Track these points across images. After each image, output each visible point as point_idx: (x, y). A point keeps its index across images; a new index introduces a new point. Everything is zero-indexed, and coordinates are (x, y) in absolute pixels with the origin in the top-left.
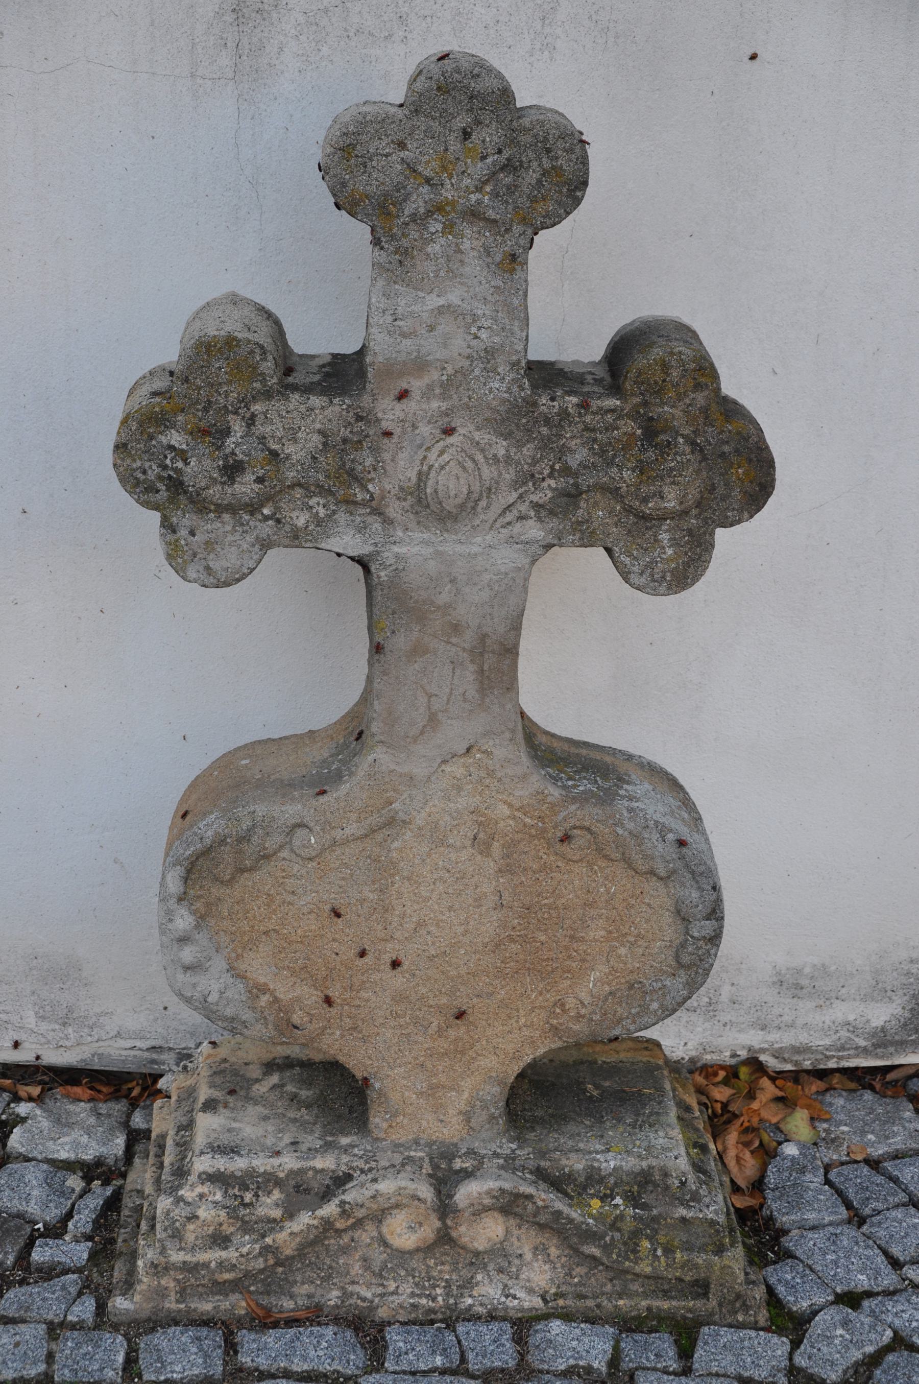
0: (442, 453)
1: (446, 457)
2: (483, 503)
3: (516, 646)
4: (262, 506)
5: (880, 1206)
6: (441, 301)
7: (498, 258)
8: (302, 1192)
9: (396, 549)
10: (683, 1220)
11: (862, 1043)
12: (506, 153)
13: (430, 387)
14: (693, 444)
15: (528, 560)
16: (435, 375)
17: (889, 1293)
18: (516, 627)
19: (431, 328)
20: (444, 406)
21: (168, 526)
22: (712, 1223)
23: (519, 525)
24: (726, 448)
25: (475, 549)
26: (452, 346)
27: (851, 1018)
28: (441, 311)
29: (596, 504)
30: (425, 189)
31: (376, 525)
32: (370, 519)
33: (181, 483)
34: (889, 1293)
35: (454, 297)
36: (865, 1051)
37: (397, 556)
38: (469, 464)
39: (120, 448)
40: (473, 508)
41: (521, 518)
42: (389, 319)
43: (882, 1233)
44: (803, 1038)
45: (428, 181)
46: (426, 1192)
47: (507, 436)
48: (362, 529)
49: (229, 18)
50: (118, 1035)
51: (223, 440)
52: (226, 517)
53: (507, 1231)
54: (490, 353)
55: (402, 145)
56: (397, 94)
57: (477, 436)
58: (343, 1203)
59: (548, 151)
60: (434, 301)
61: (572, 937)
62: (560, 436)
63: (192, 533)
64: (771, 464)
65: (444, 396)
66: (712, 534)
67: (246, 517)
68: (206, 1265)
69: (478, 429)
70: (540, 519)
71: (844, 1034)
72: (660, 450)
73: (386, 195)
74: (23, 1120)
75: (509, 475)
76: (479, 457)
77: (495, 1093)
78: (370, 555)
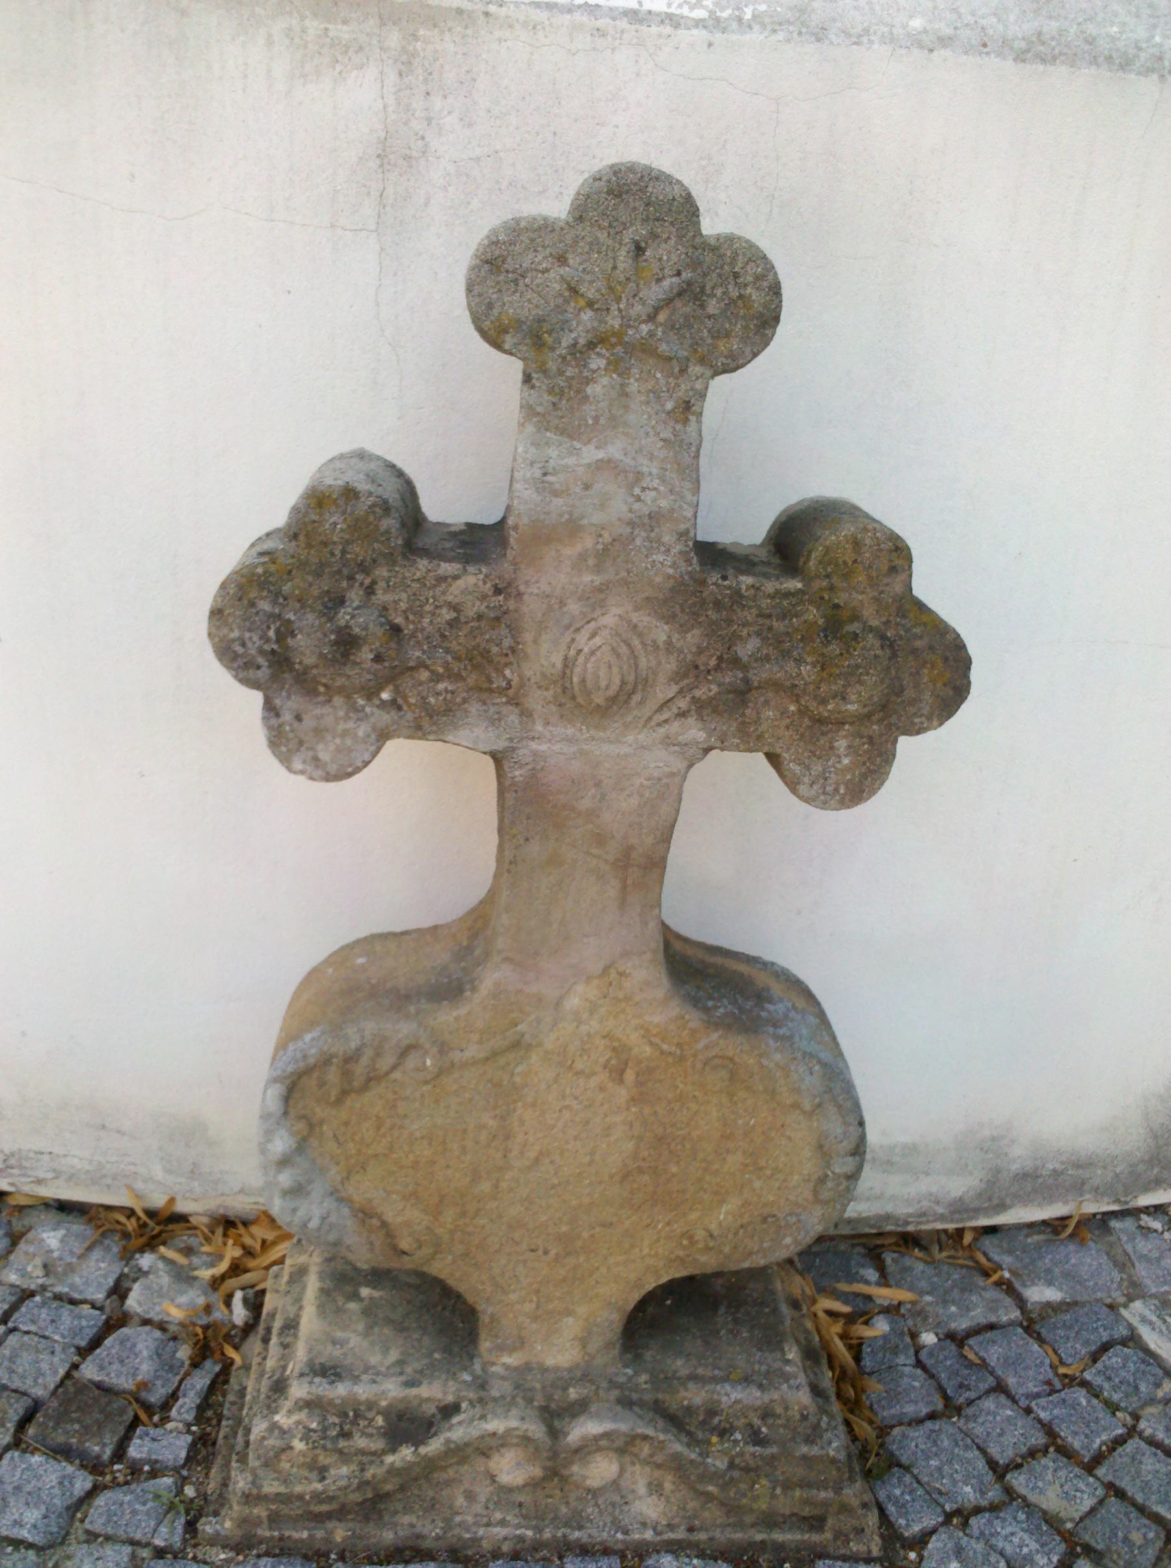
0: (593, 635)
1: (597, 641)
2: (637, 698)
3: (664, 859)
4: (381, 689)
5: (972, 1395)
6: (601, 455)
7: (669, 406)
8: (407, 1426)
9: (534, 745)
10: (805, 1458)
11: (940, 1210)
12: (687, 275)
13: (583, 557)
14: (883, 637)
15: (685, 764)
16: (589, 542)
17: (993, 1508)
18: (666, 838)
19: (587, 487)
20: (598, 580)
21: (270, 708)
22: (833, 1461)
23: (676, 724)
24: (918, 644)
25: (625, 750)
26: (614, 507)
27: (934, 1189)
28: (600, 466)
29: (767, 702)
30: (587, 316)
31: (513, 717)
32: (505, 710)
33: (287, 660)
34: (993, 1508)
35: (614, 450)
36: (942, 1218)
37: (535, 754)
38: (624, 650)
39: (216, 613)
40: (626, 702)
41: (682, 714)
42: (538, 473)
43: (979, 1430)
44: (889, 1208)
45: (590, 304)
46: (536, 1429)
47: (670, 619)
48: (495, 721)
49: (374, 164)
50: (242, 1191)
51: (346, 613)
52: (338, 700)
53: (622, 1471)
54: (655, 518)
55: (562, 260)
56: (558, 208)
57: (635, 617)
58: (448, 1441)
59: (736, 276)
60: (591, 454)
61: (705, 1170)
62: (730, 622)
63: (298, 718)
64: (967, 663)
65: (598, 569)
66: (895, 741)
67: (361, 702)
68: (300, 1497)
69: (637, 608)
70: (701, 718)
71: (925, 1204)
72: (831, 643)
73: (540, 321)
74: (146, 1273)
75: (670, 665)
76: (636, 642)
77: (611, 1320)
78: (504, 751)
